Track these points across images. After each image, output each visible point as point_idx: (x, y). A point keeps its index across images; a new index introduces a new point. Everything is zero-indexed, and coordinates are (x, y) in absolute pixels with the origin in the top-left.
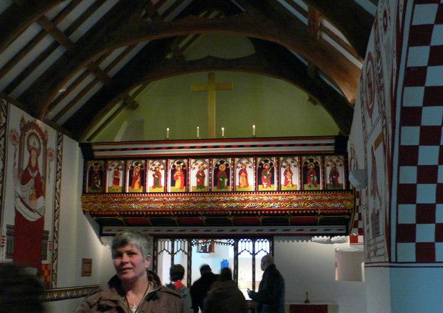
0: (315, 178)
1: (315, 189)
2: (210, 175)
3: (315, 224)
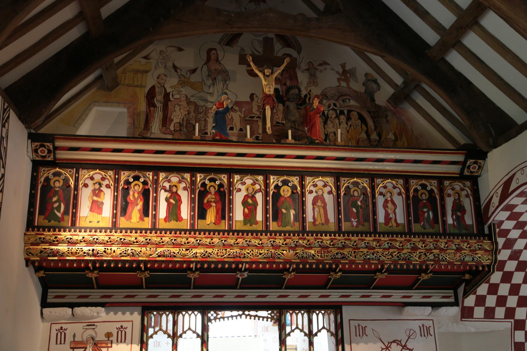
0: (431, 213)
1: (431, 231)
2: (266, 203)
3: (410, 288)
